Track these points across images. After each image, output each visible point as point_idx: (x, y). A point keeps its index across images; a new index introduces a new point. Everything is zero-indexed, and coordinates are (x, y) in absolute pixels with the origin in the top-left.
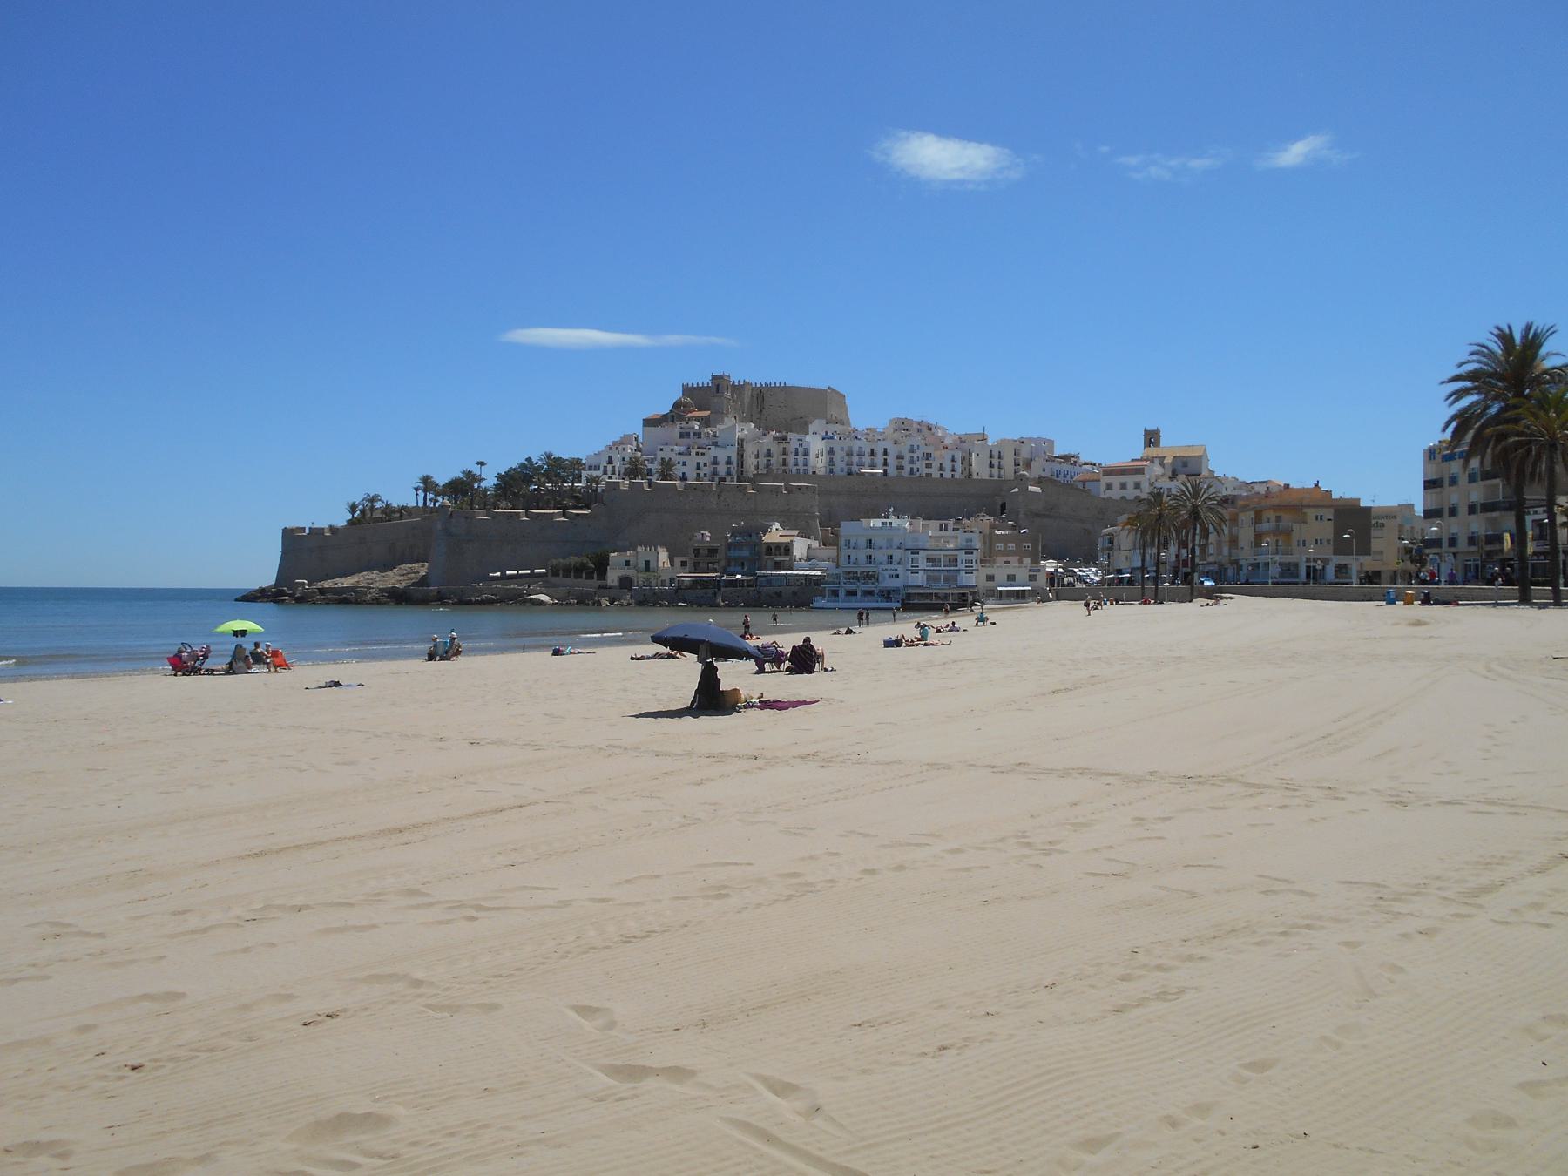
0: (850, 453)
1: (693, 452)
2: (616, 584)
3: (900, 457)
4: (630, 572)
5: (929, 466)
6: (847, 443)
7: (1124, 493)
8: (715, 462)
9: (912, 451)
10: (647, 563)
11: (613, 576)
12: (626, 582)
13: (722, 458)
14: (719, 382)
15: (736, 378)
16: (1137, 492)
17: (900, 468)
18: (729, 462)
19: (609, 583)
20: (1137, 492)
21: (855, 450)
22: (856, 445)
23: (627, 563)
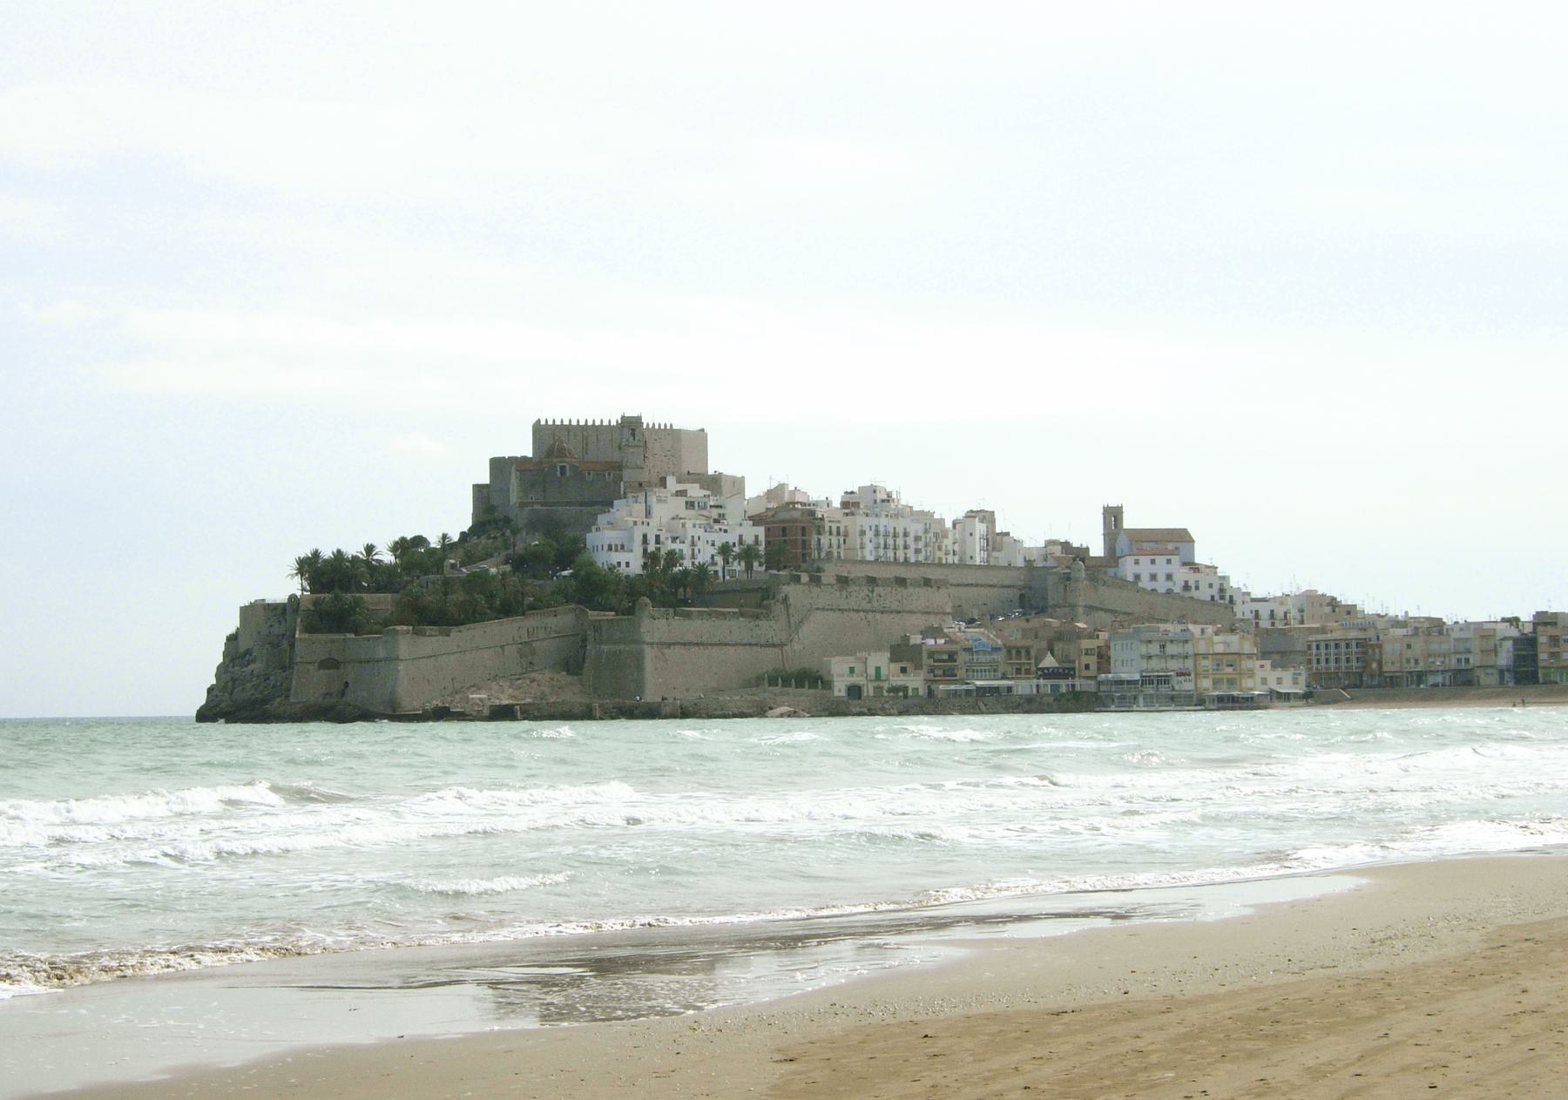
0: (877, 534)
2: (843, 693)
3: (917, 539)
4: (857, 680)
5: (940, 548)
7: (1153, 585)
9: (926, 531)
10: (878, 669)
11: (839, 689)
12: (855, 691)
14: (631, 426)
16: (1169, 585)
17: (917, 551)
19: (836, 693)
20: (1169, 585)
21: (881, 529)
22: (883, 521)
23: (852, 670)
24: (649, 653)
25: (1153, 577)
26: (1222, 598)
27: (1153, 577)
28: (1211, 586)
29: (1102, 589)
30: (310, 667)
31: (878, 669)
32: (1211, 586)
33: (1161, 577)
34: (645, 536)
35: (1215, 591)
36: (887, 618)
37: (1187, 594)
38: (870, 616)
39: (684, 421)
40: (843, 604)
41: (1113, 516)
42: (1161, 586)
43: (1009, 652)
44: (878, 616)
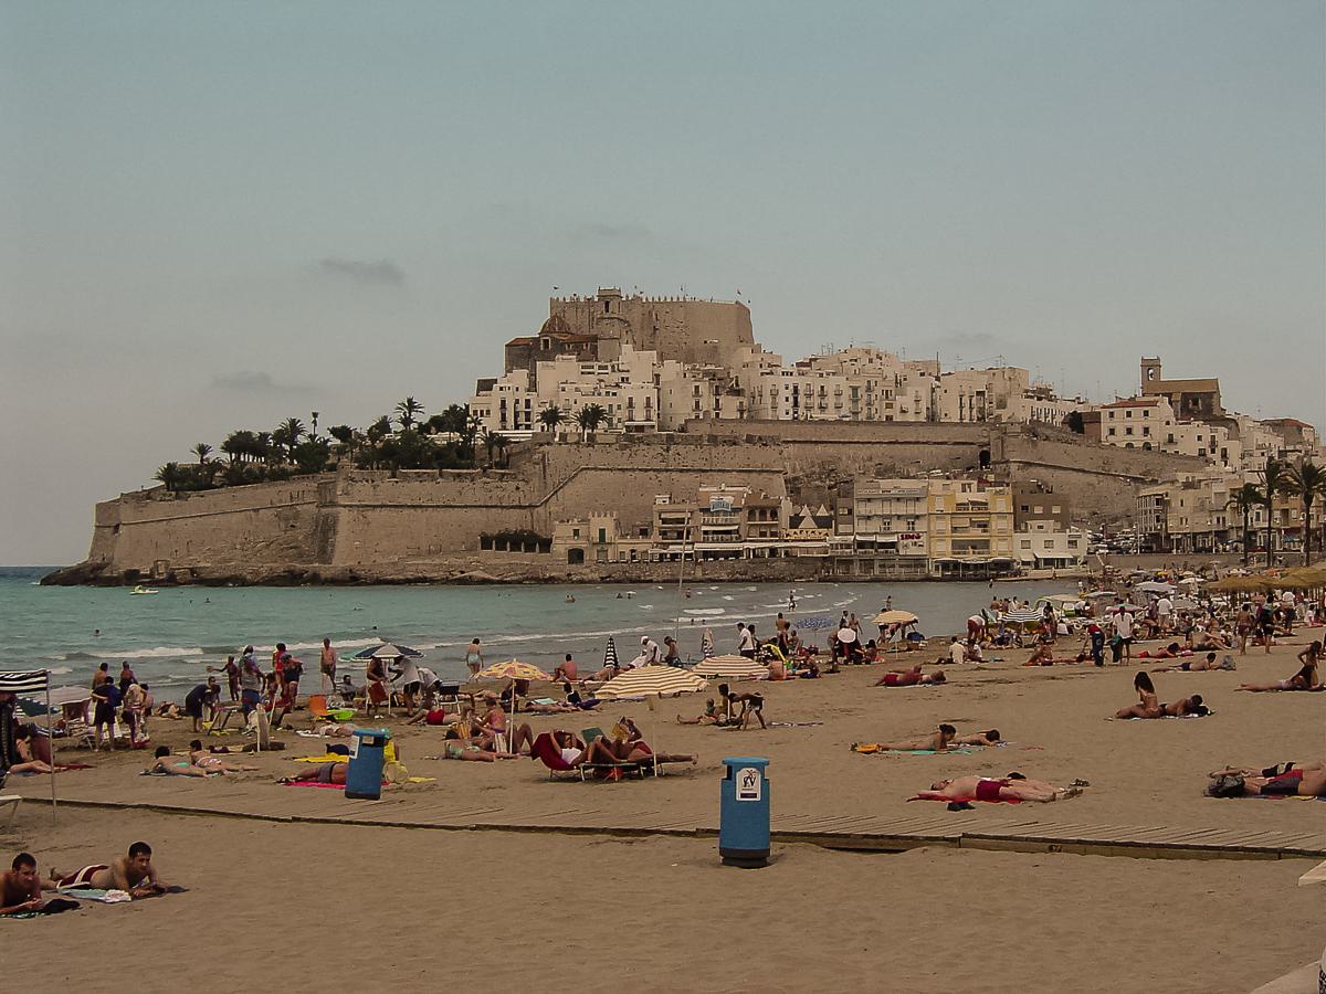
0: (796, 390)
1: (603, 392)
4: (580, 544)
6: (790, 381)
8: (631, 405)
10: (602, 532)
12: (576, 556)
13: (639, 403)
15: (627, 292)
18: (648, 405)
24: (344, 516)
25: (1129, 431)
26: (1213, 451)
27: (1129, 431)
28: (1199, 438)
29: (1041, 444)
30: (106, 530)
31: (602, 532)
32: (1199, 438)
33: (1138, 431)
34: (503, 402)
35: (1205, 444)
36: (685, 478)
37: (1171, 450)
38: (662, 476)
39: (720, 292)
40: (1043, 471)
41: (1150, 366)
42: (1138, 440)
43: (751, 513)
44: (675, 475)
